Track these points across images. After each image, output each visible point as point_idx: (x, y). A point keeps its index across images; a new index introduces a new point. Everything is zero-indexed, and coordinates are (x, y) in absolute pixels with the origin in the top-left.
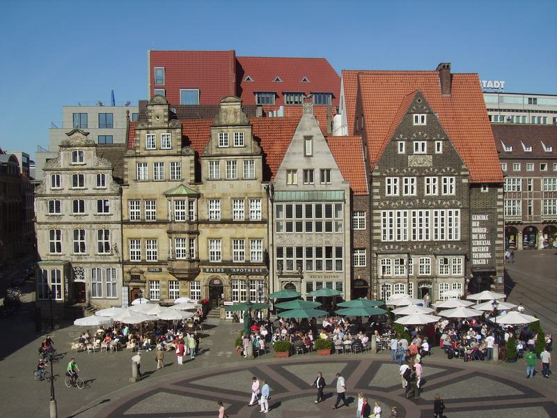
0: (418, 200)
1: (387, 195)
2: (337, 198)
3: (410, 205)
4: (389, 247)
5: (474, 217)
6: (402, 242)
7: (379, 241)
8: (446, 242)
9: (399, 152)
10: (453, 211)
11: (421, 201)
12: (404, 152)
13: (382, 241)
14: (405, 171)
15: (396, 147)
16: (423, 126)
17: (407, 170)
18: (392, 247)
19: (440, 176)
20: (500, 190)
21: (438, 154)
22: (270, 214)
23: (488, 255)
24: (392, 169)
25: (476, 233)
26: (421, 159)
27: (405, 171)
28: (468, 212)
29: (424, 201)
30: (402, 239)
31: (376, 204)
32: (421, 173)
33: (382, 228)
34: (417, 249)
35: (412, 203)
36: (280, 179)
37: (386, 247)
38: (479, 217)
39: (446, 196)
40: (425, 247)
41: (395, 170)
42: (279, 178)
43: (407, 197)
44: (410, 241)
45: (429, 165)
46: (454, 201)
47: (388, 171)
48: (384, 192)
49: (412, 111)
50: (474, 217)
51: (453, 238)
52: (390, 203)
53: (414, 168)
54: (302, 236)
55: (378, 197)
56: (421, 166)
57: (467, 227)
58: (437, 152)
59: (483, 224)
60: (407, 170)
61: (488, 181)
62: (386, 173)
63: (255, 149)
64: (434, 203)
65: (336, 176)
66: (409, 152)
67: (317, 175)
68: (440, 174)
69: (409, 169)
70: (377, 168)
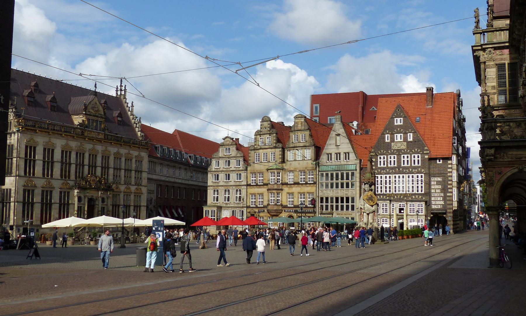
0: (397, 169)
1: (379, 166)
2: (352, 169)
4: (380, 197)
5: (432, 179)
6: (388, 194)
8: (415, 194)
9: (387, 141)
10: (420, 175)
11: (399, 169)
12: (389, 141)
14: (389, 152)
15: (384, 138)
16: (400, 125)
17: (391, 151)
18: (382, 197)
19: (411, 155)
20: (449, 162)
22: (317, 179)
23: (442, 203)
24: (382, 151)
25: (434, 189)
27: (389, 152)
28: (429, 175)
30: (388, 192)
32: (399, 153)
35: (394, 171)
36: (324, 158)
38: (436, 179)
39: (415, 166)
40: (402, 197)
41: (383, 151)
42: (322, 159)
43: (391, 167)
44: (393, 193)
45: (405, 148)
46: (419, 169)
47: (380, 152)
48: (377, 164)
49: (394, 117)
50: (432, 179)
51: (420, 192)
52: (381, 171)
54: (333, 191)
56: (399, 148)
57: (428, 185)
58: (409, 140)
59: (438, 183)
60: (391, 151)
61: (442, 157)
62: (378, 153)
63: (311, 142)
64: (407, 171)
65: (352, 156)
66: (392, 140)
67: (342, 156)
68: (411, 153)
69: (392, 151)
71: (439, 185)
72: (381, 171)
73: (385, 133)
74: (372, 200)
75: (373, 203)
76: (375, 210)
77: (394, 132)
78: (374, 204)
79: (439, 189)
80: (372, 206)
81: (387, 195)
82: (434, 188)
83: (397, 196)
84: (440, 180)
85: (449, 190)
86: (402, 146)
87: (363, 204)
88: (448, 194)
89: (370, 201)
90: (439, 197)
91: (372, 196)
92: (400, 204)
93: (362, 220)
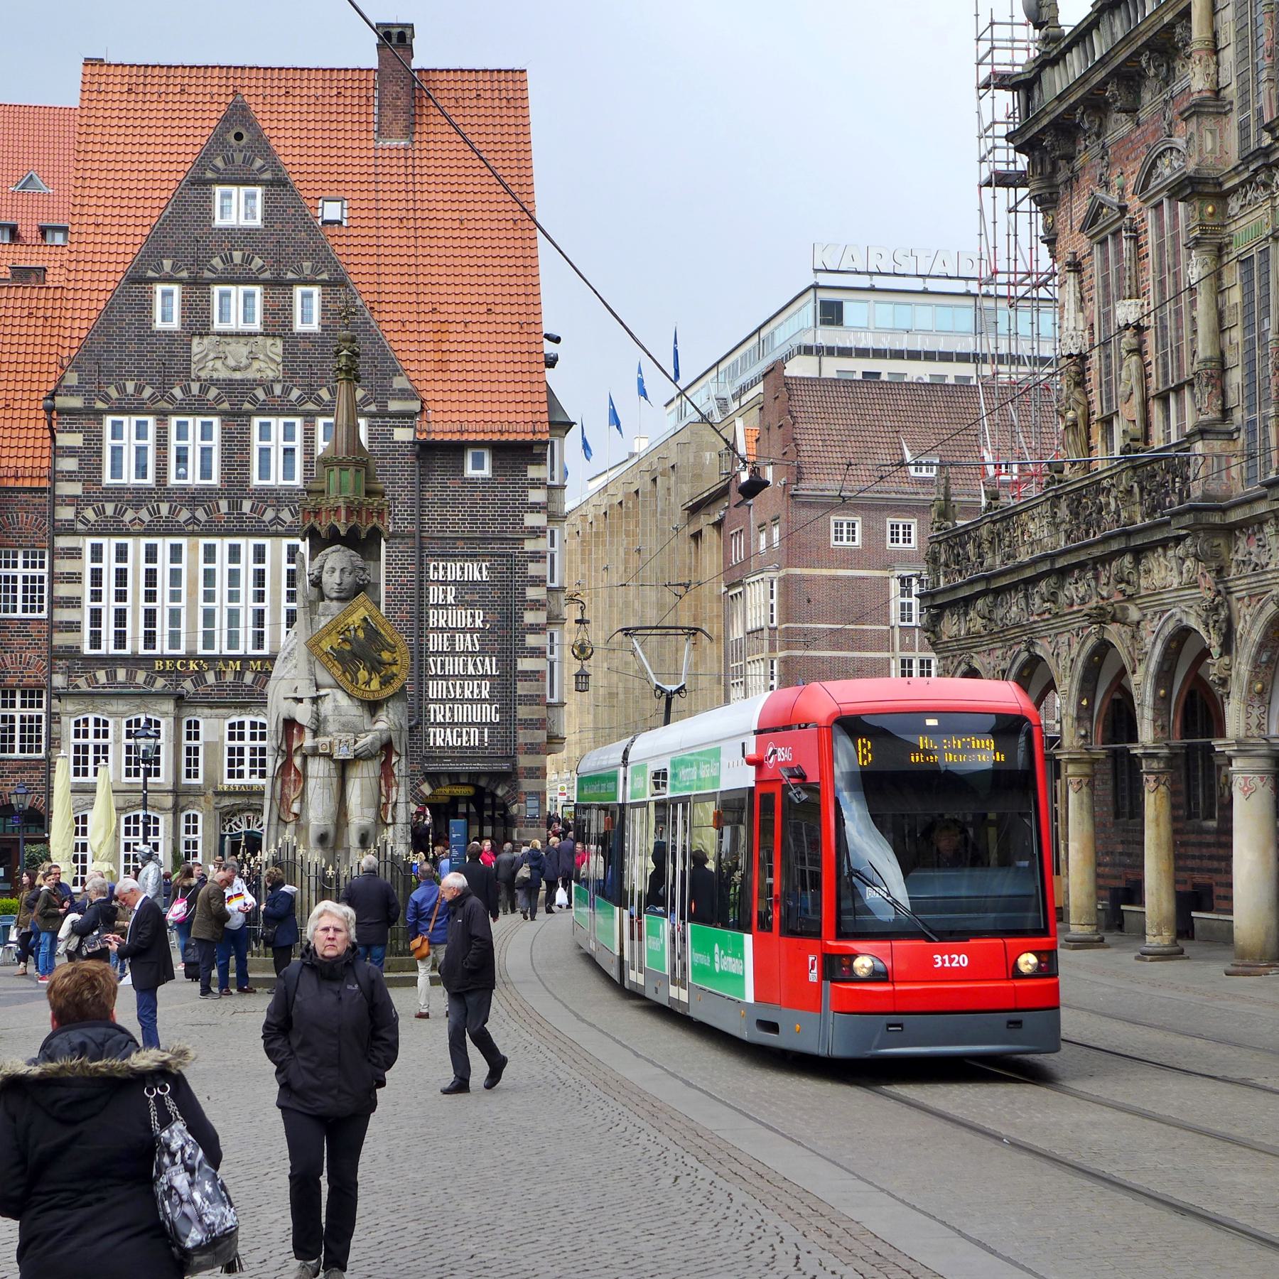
0: (224, 505)
1: (107, 479)
3: (194, 520)
4: (112, 676)
6: (163, 658)
7: (72, 653)
9: (159, 325)
11: (235, 505)
12: (175, 324)
13: (87, 650)
14: (177, 392)
15: (145, 307)
16: (249, 232)
17: (186, 390)
18: (121, 674)
20: (533, 472)
21: (305, 336)
23: (489, 713)
24: (130, 387)
25: (442, 630)
26: (239, 351)
27: (177, 392)
29: (247, 506)
30: (162, 646)
31: (66, 513)
33: (88, 604)
34: (220, 686)
35: (201, 514)
37: (101, 676)
38: (454, 570)
40: (249, 678)
41: (139, 389)
43: (183, 489)
44: (191, 656)
45: (271, 375)
47: (114, 393)
48: (99, 469)
49: (209, 175)
52: (119, 512)
53: (213, 382)
55: (75, 489)
56: (238, 376)
58: (299, 327)
59: (468, 593)
61: (496, 437)
62: (106, 398)
66: (197, 320)
68: (310, 406)
69: (195, 388)
70: (72, 379)
71: (471, 605)
72: (119, 512)
73: (150, 274)
74: (376, 666)
75: (385, 682)
76: (394, 736)
77: (207, 274)
78: (389, 691)
79: (472, 630)
80: (373, 707)
81: (158, 665)
82: (442, 623)
83: (219, 674)
84: (477, 576)
85: (531, 640)
86: (256, 365)
87: (307, 692)
88: (525, 664)
89: (363, 675)
90: (472, 677)
91: (372, 633)
92: (235, 719)
93: (295, 808)
